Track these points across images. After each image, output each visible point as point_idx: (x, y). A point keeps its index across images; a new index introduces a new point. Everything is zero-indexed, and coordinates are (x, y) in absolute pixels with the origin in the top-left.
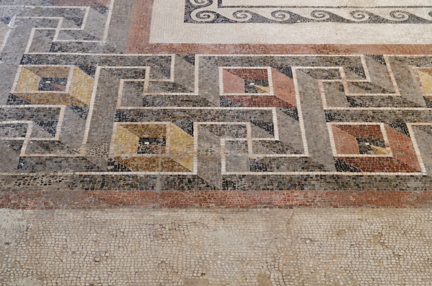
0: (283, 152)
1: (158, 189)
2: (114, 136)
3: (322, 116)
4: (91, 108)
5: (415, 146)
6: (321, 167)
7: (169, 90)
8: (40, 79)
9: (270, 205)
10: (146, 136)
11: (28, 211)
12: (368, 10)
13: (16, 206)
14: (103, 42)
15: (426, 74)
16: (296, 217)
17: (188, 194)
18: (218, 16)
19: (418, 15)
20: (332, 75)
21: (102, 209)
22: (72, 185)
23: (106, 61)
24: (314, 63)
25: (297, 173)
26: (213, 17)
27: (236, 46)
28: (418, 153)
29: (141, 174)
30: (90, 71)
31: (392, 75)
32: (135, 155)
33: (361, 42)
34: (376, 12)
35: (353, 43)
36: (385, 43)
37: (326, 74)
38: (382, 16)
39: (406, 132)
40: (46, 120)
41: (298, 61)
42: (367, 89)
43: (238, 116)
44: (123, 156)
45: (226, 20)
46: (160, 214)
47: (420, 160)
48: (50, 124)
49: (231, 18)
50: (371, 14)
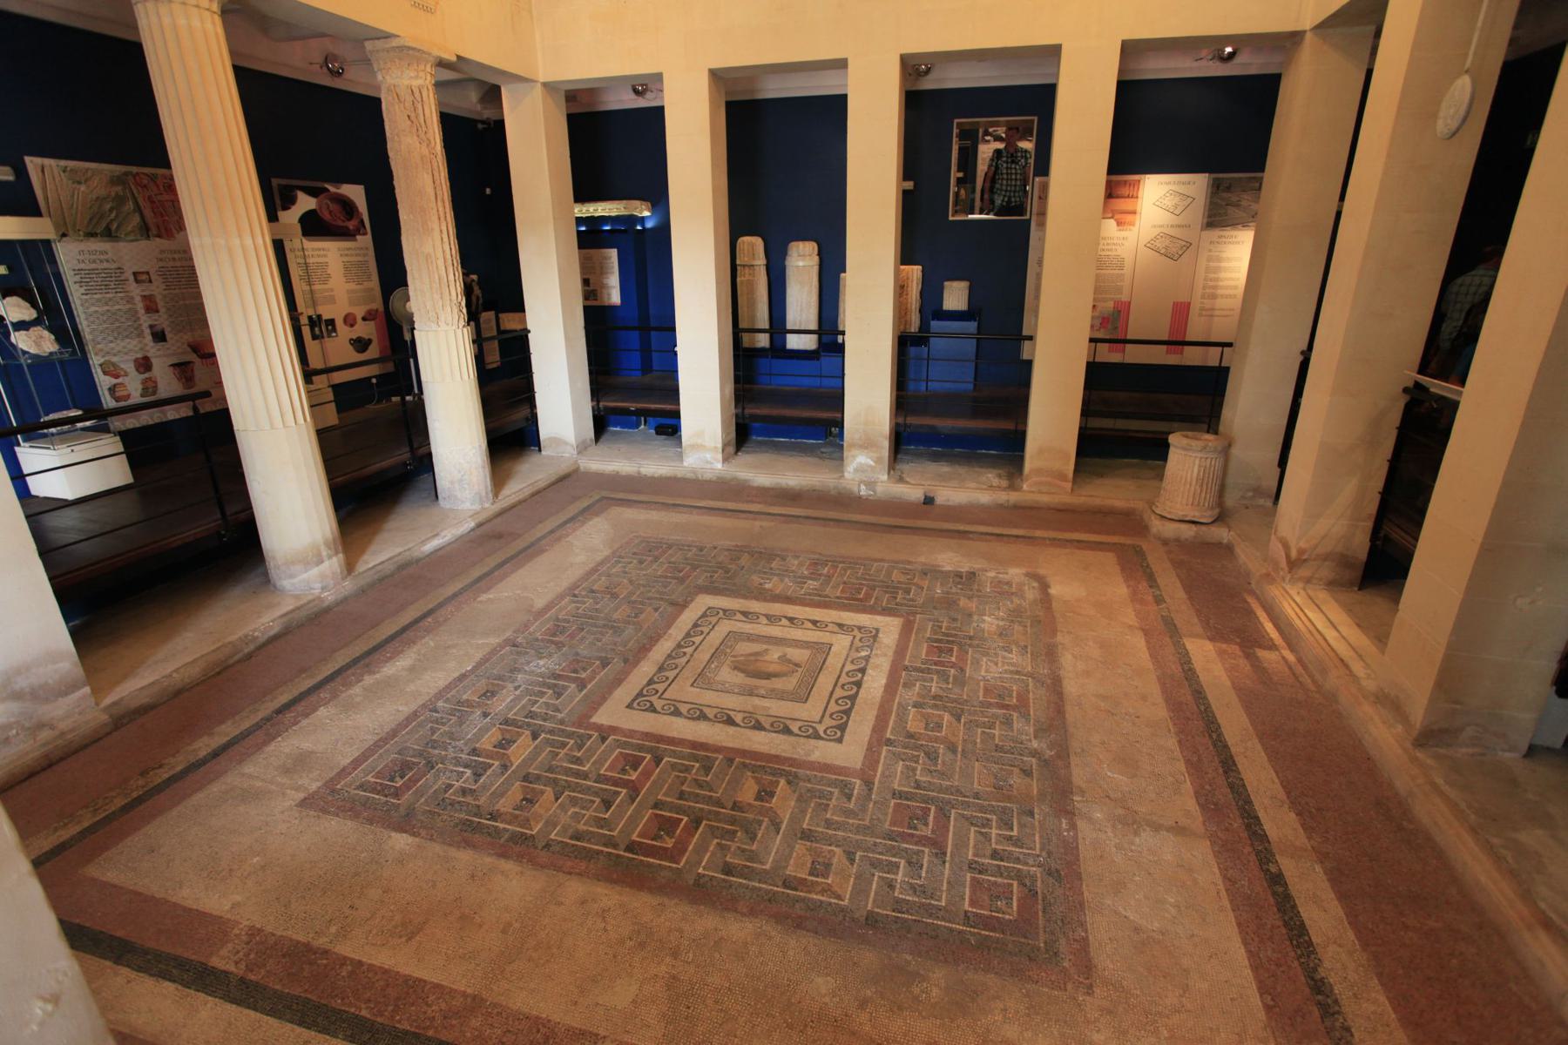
0: (602, 828)
1: (503, 840)
2: (510, 792)
3: (652, 803)
4: (514, 767)
5: (695, 840)
6: (615, 846)
7: (572, 763)
8: (500, 738)
9: (559, 869)
10: (528, 796)
11: (417, 840)
12: (759, 717)
13: (414, 835)
14: (560, 716)
15: (753, 781)
16: (567, 883)
17: (517, 849)
18: (652, 705)
19: (791, 727)
20: (687, 769)
21: (458, 847)
22: (456, 825)
23: (551, 732)
24: (683, 758)
25: (596, 847)
26: (648, 704)
27: (643, 733)
28: (691, 848)
29: (501, 826)
30: (535, 736)
31: (727, 778)
32: (510, 810)
33: (731, 745)
34: (762, 720)
35: (724, 744)
36: (746, 748)
37: (683, 768)
38: (763, 723)
39: (697, 828)
40: (480, 771)
41: (674, 754)
42: (701, 787)
43: (596, 794)
44: (502, 809)
45: (654, 711)
46: (488, 860)
47: (687, 854)
48: (480, 775)
49: (659, 709)
50: (757, 721)
